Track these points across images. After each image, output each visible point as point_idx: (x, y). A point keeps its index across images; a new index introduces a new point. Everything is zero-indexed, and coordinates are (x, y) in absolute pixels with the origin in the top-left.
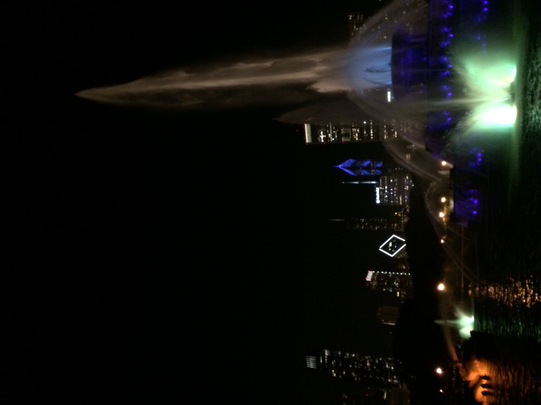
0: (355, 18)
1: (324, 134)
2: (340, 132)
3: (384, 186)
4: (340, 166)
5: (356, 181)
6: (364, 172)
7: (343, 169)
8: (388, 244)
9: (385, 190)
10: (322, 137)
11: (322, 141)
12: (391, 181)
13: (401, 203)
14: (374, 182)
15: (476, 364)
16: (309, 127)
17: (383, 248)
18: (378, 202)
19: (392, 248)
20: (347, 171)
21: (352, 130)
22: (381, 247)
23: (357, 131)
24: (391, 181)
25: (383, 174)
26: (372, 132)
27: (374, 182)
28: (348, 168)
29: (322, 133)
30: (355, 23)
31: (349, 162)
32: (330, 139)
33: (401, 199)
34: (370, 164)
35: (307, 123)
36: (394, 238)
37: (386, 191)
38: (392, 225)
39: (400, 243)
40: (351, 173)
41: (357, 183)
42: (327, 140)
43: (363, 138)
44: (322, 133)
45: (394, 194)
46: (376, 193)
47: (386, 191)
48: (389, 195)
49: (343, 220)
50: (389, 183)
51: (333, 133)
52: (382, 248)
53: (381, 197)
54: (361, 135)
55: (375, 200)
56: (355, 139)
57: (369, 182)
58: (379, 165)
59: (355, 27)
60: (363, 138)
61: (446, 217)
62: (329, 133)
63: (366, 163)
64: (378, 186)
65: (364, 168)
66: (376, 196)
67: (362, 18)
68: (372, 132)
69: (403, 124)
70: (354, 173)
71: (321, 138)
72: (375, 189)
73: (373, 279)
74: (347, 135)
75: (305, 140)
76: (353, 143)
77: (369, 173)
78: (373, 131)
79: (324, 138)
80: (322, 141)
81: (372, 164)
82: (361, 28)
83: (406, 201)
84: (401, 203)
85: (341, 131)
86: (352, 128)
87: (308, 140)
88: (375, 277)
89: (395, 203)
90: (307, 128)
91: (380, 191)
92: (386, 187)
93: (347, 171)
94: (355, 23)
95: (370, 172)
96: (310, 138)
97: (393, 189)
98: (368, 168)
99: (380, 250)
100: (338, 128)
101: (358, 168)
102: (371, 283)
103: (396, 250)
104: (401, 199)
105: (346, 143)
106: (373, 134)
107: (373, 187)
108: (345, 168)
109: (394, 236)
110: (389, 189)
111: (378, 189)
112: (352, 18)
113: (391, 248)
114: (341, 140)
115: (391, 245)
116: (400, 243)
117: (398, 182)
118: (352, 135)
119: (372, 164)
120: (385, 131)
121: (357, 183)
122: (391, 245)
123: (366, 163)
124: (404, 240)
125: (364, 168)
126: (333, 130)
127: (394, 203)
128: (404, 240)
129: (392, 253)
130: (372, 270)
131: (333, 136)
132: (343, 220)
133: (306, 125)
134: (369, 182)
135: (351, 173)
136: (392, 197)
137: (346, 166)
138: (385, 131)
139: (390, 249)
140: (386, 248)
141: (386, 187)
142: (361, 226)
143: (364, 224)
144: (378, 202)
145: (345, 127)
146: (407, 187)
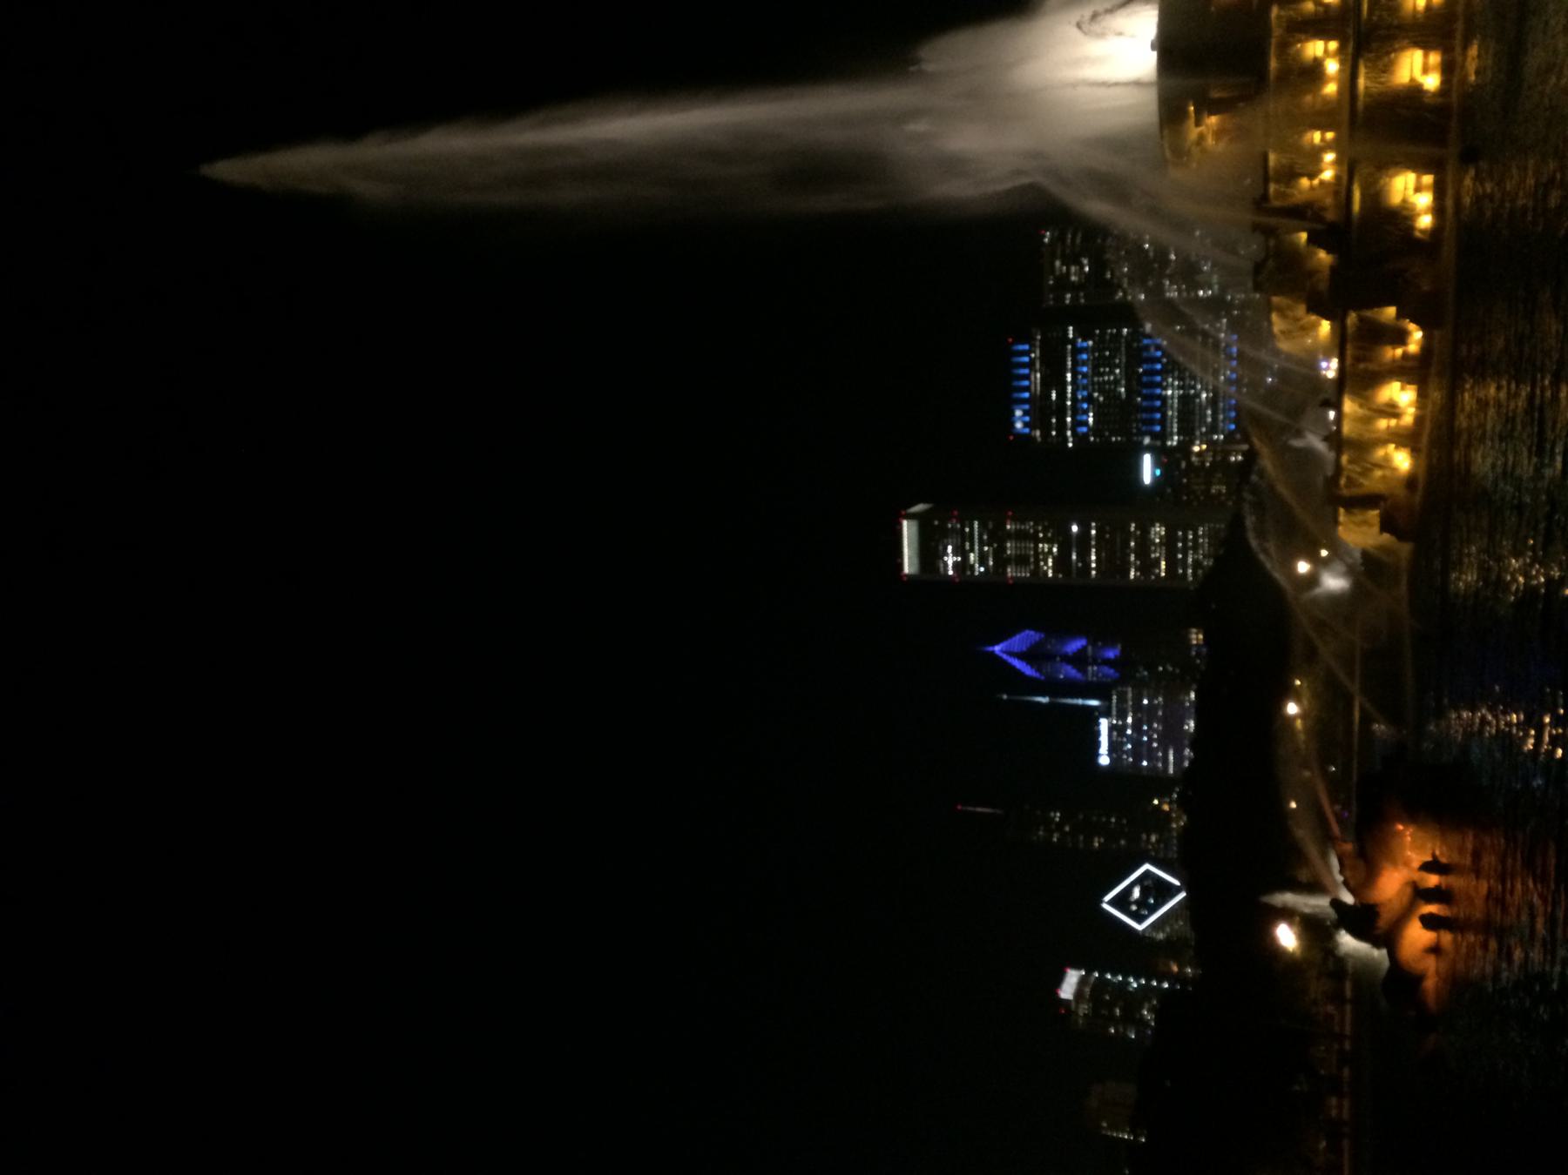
0: (1059, 239)
1: (955, 553)
2: (1002, 549)
3: (1122, 715)
4: (997, 648)
5: (1043, 695)
6: (1068, 672)
7: (1005, 656)
8: (1128, 891)
9: (1125, 726)
10: (950, 560)
11: (951, 573)
12: (1146, 702)
13: (1171, 771)
14: (1094, 703)
15: (1400, 834)
16: (915, 528)
17: (1111, 903)
18: (1104, 760)
19: (1141, 903)
20: (1017, 663)
21: (1036, 547)
22: (1108, 898)
23: (1050, 550)
24: (1146, 702)
25: (1123, 681)
26: (1093, 558)
27: (1094, 703)
28: (1021, 656)
29: (950, 548)
30: (1059, 252)
31: (1024, 639)
32: (972, 567)
33: (1171, 758)
34: (1084, 648)
35: (910, 517)
36: (1147, 873)
37: (1129, 732)
38: (1144, 836)
39: (1165, 891)
40: (1028, 670)
41: (1044, 700)
42: (964, 571)
43: (1067, 573)
44: (950, 548)
45: (1151, 740)
46: (1098, 734)
47: (1129, 732)
48: (1137, 743)
49: (999, 811)
50: (1138, 707)
51: (981, 550)
52: (1111, 903)
53: (1114, 748)
54: (1062, 562)
55: (1097, 755)
56: (1046, 573)
57: (1080, 702)
58: (1111, 654)
59: (1058, 263)
60: (1067, 573)
61: (1304, 716)
62: (972, 550)
63: (1075, 645)
64: (1107, 715)
65: (1067, 659)
66: (1097, 745)
67: (1078, 241)
68: (1093, 558)
69: (1185, 540)
70: (1039, 670)
71: (946, 564)
72: (1098, 724)
73: (1079, 994)
74: (1021, 560)
75: (901, 566)
76: (1037, 583)
77: (1079, 676)
78: (1097, 554)
79: (955, 564)
80: (951, 573)
81: (1090, 649)
82: (1073, 269)
83: (1186, 764)
84: (1171, 771)
85: (1005, 549)
86: (1037, 541)
87: (909, 565)
88: (1087, 990)
89: (1155, 767)
90: (908, 529)
91: (1112, 728)
92: (1130, 720)
93: (1017, 663)
94: (1059, 252)
95: (1085, 672)
96: (916, 561)
97: (1150, 727)
98: (1079, 660)
99: (1106, 906)
100: (997, 537)
101: (1050, 657)
102: (1073, 1006)
103: (1153, 909)
104: (1171, 758)
105: (1019, 584)
106: (1097, 561)
107: (1091, 717)
108: (1010, 654)
109: (1147, 867)
110: (1136, 726)
111: (1104, 724)
112: (1051, 239)
113: (1137, 902)
114: (1005, 572)
115: (1136, 893)
116: (1165, 891)
117: (1165, 707)
118: (1037, 561)
119: (1090, 649)
120: (1132, 558)
121: (1044, 700)
122: (1136, 893)
123: (1075, 645)
124: (1177, 883)
125: (1067, 659)
126: (982, 544)
127: (1151, 768)
128: (1177, 883)
129: (1139, 918)
130: (1077, 967)
131: (983, 560)
132: (999, 811)
133: (905, 523)
134: (1080, 702)
135: (1028, 670)
136: (1144, 750)
137: (1016, 649)
138: (1132, 558)
139: (1134, 908)
140: (1122, 902)
141: (1130, 720)
142: (1051, 833)
143: (1060, 826)
144: (1104, 760)
145: (1020, 536)
146: (1192, 724)
